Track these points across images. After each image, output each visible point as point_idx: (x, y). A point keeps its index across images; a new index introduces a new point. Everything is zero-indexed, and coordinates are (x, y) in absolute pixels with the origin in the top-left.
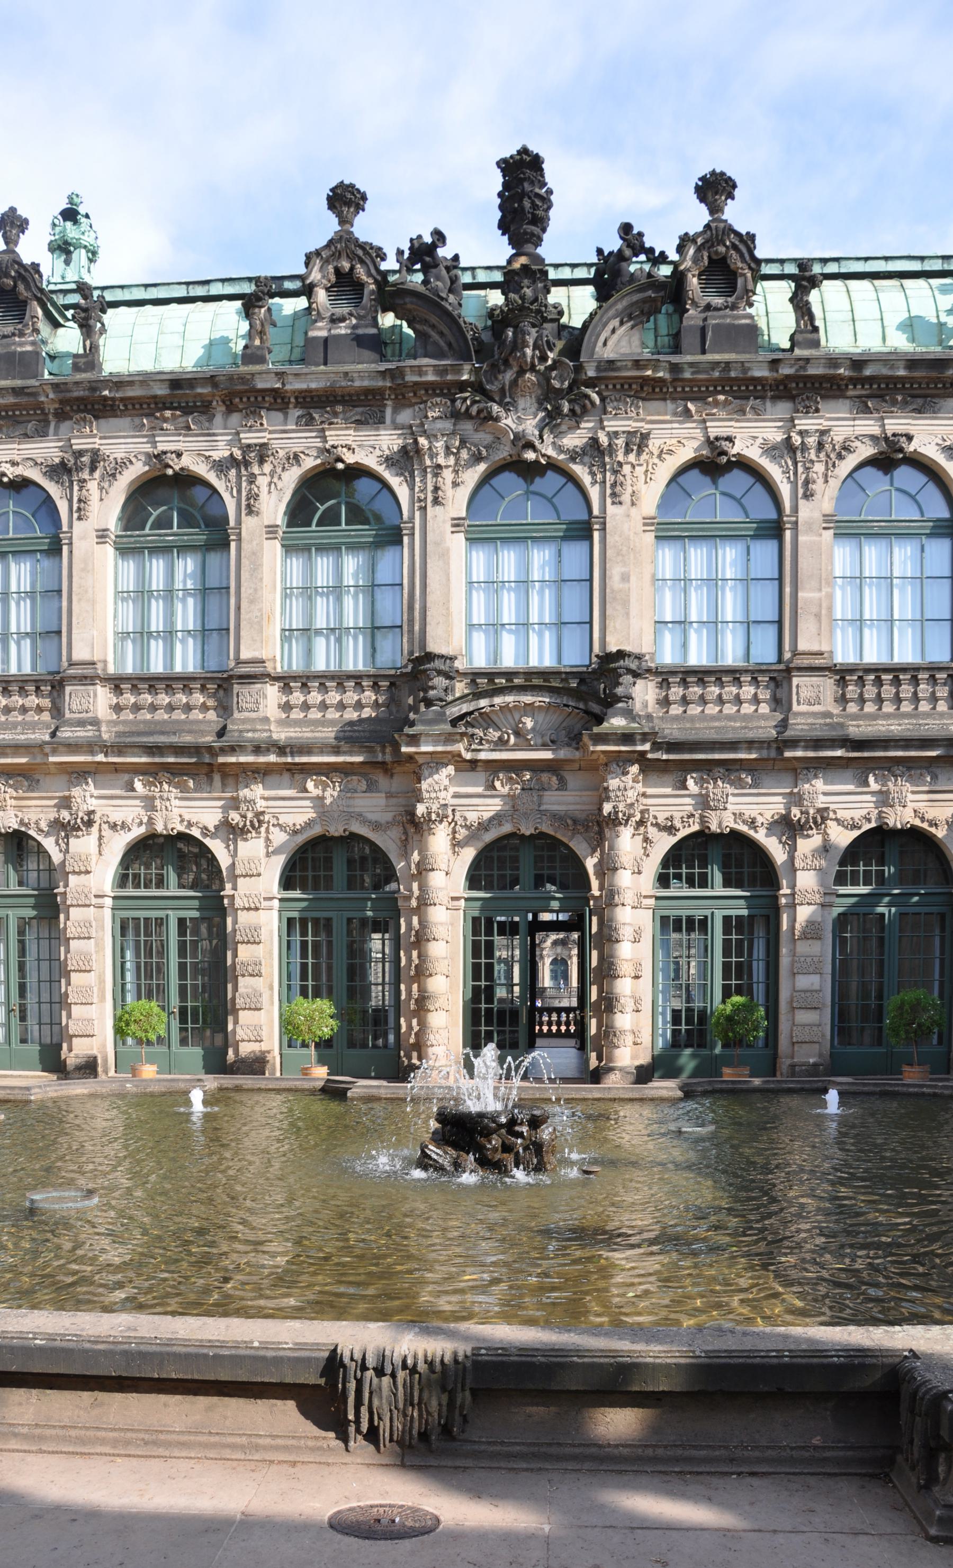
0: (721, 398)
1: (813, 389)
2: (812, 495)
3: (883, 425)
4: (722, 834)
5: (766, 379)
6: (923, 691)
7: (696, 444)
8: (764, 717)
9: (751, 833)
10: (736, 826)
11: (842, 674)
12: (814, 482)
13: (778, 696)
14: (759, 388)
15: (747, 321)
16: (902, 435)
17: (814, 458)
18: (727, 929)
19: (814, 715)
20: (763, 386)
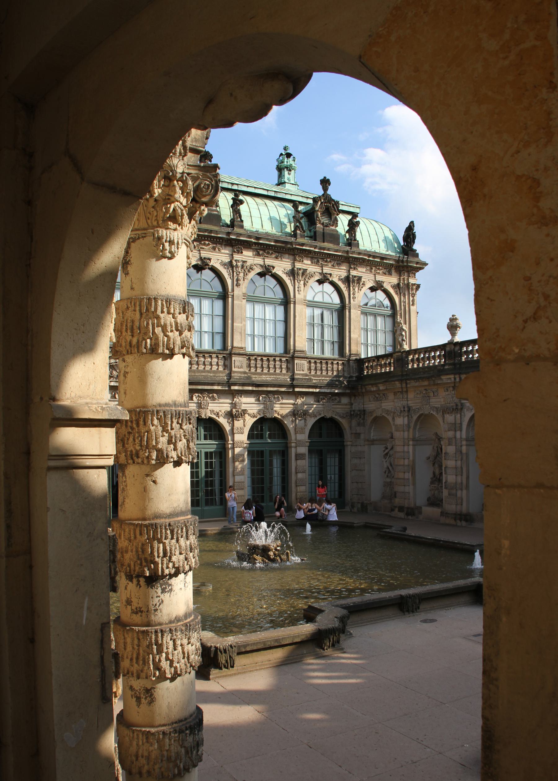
0: (207, 242)
1: (241, 245)
2: (239, 285)
3: (264, 261)
4: (206, 419)
5: (224, 238)
6: (278, 365)
7: (196, 259)
8: (221, 372)
9: (217, 418)
10: (211, 416)
11: (249, 356)
12: (240, 280)
13: (226, 364)
14: (221, 241)
15: (216, 213)
16: (271, 266)
17: (240, 271)
18: (206, 458)
19: (241, 372)
20: (222, 240)
